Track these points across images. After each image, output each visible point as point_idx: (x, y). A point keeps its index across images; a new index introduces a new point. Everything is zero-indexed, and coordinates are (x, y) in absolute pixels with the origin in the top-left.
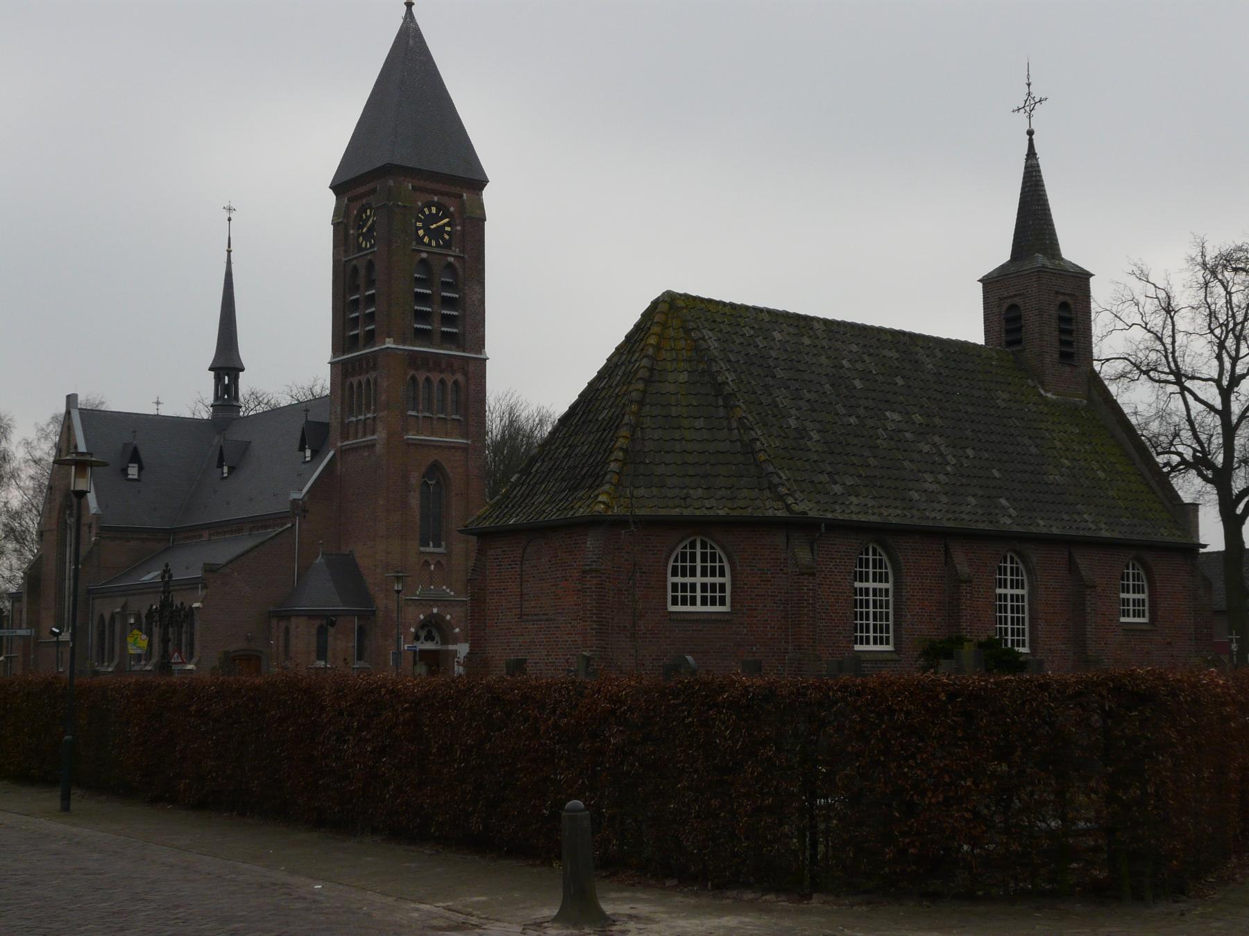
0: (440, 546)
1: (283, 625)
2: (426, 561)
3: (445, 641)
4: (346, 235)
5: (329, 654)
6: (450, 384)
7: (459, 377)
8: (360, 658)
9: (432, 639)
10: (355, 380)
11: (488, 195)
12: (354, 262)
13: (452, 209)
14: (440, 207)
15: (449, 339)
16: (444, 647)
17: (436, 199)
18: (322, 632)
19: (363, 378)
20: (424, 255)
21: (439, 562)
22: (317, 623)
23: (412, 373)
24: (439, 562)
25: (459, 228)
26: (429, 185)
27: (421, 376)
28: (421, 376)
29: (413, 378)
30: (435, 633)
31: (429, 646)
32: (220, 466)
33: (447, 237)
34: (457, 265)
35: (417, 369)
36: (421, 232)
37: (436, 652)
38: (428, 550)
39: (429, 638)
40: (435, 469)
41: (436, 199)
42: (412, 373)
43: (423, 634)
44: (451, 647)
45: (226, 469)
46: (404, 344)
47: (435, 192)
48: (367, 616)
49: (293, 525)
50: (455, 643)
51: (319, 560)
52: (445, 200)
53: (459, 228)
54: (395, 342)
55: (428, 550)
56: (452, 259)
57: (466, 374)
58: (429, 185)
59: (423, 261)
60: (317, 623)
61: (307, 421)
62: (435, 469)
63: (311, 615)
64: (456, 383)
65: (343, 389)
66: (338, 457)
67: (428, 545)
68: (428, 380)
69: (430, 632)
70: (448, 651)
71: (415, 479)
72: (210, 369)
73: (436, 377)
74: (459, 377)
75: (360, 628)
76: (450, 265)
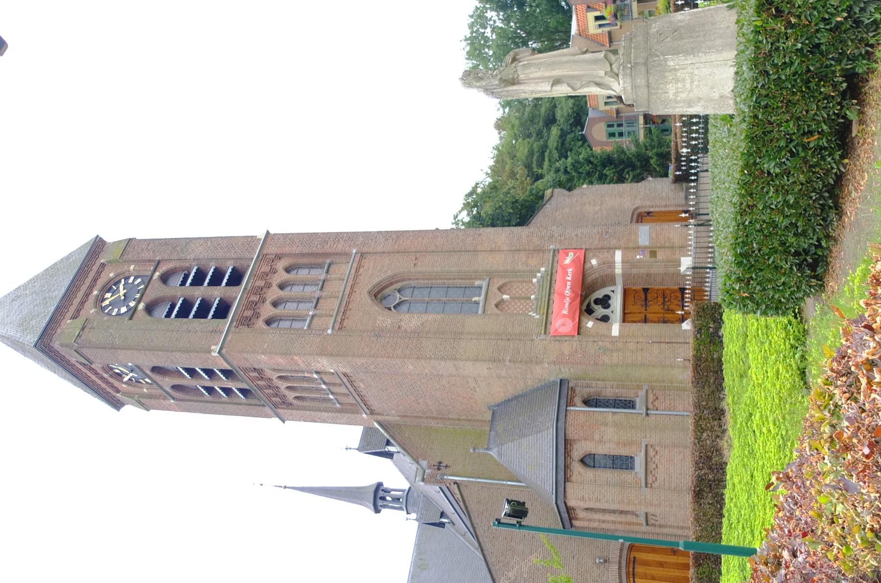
0: (481, 288)
1: (581, 514)
2: (497, 306)
3: (610, 280)
4: (150, 396)
5: (624, 452)
6: (285, 276)
7: (281, 265)
8: (629, 404)
9: (607, 297)
10: (291, 396)
11: (110, 237)
12: (168, 389)
13: (112, 275)
14: (107, 288)
15: (236, 278)
16: (619, 281)
17: (95, 293)
18: (588, 461)
19: (282, 385)
20: (141, 306)
21: (499, 289)
22: (577, 468)
23: (260, 323)
24: (499, 289)
25: (132, 267)
26: (76, 301)
27: (267, 311)
28: (267, 311)
29: (268, 322)
30: (599, 294)
31: (617, 302)
32: (442, 525)
33: (139, 280)
34: (163, 269)
35: (258, 316)
36: (124, 310)
37: (626, 292)
38: (481, 304)
39: (605, 302)
40: (378, 294)
41: (95, 293)
42: (260, 323)
43: (600, 311)
44: (618, 270)
45: (443, 520)
46: (222, 333)
47: (87, 295)
48: (565, 392)
49: (455, 483)
50: (612, 264)
51: (493, 453)
52: (100, 283)
53: (132, 267)
54: (216, 344)
55: (481, 304)
56: (157, 274)
57: (279, 257)
58: (76, 301)
59: (149, 309)
60: (577, 468)
61: (358, 449)
62: (378, 294)
63: (564, 475)
64: (288, 270)
65: (304, 408)
66: (380, 418)
67: (477, 303)
68: (275, 304)
69: (597, 302)
70: (624, 275)
71: (385, 319)
72: (377, 511)
73: (274, 293)
74: (281, 265)
75: (587, 402)
76: (165, 279)
